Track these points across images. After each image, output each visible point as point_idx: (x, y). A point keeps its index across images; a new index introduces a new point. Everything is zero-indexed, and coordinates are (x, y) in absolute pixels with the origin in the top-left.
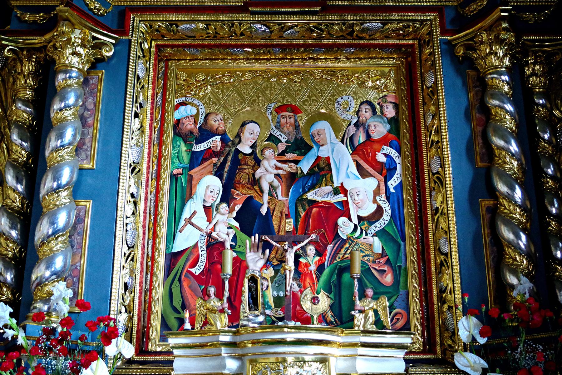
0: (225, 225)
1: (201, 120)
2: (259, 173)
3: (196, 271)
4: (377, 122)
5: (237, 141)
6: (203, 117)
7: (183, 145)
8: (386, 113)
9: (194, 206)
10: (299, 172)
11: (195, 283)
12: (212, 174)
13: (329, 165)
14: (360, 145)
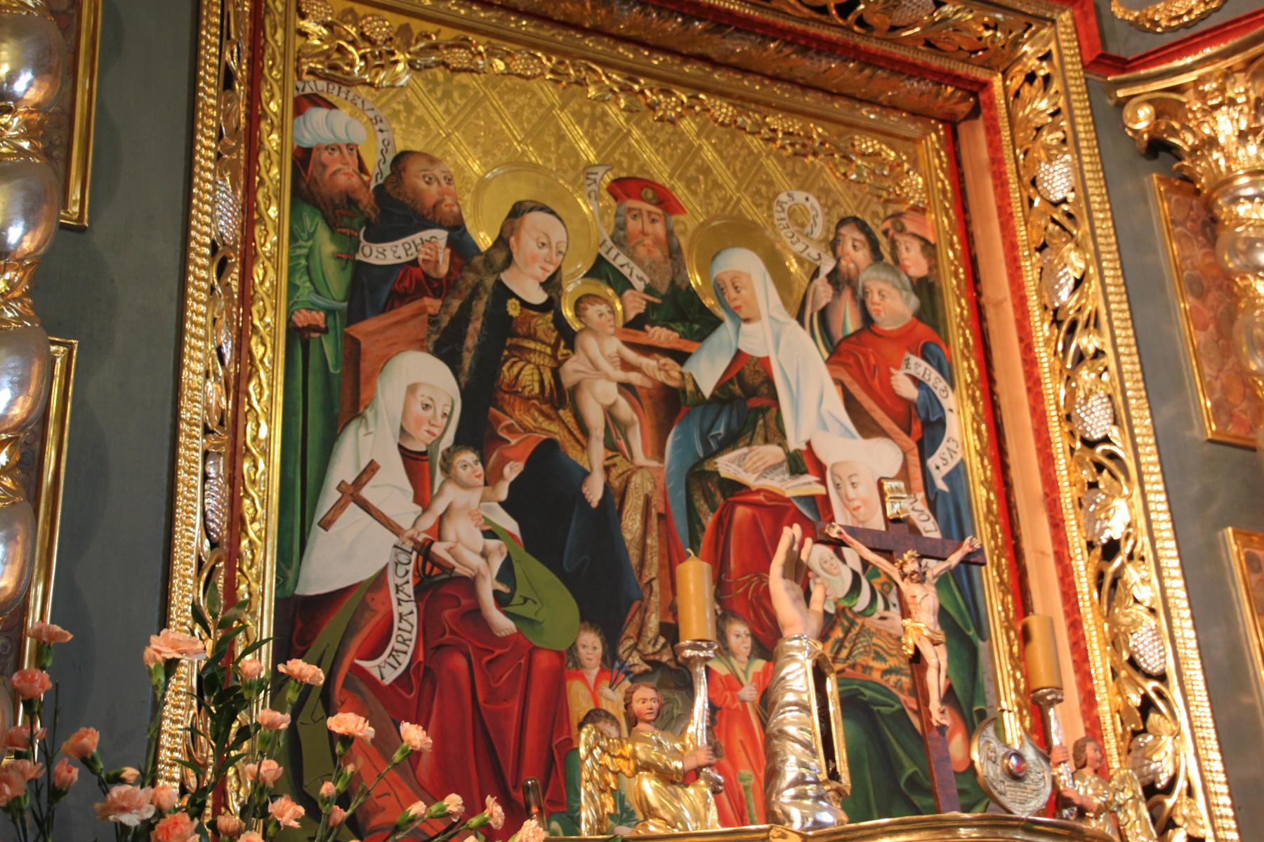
0: (475, 526)
2: (573, 369)
4: (886, 281)
5: (500, 257)
6: (390, 158)
8: (907, 263)
9: (367, 445)
10: (690, 388)
12: (423, 348)
13: (770, 382)
14: (847, 338)
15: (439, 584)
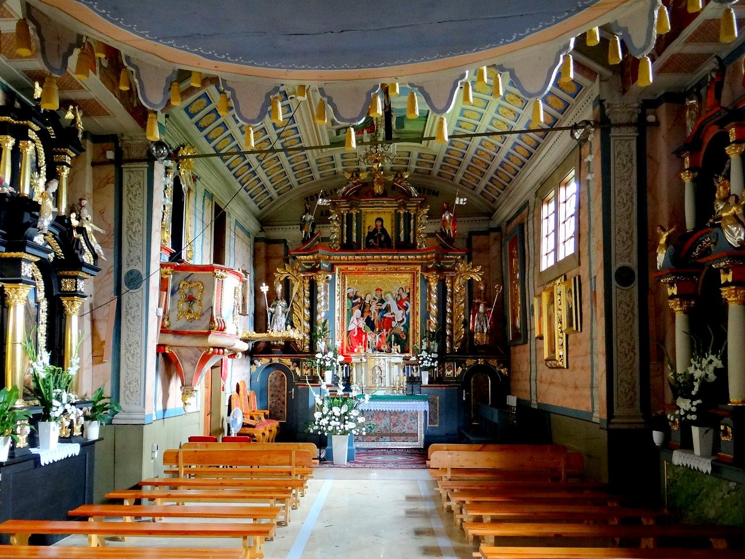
0: (362, 324)
1: (354, 294)
3: (355, 335)
9: (353, 318)
15: (359, 329)
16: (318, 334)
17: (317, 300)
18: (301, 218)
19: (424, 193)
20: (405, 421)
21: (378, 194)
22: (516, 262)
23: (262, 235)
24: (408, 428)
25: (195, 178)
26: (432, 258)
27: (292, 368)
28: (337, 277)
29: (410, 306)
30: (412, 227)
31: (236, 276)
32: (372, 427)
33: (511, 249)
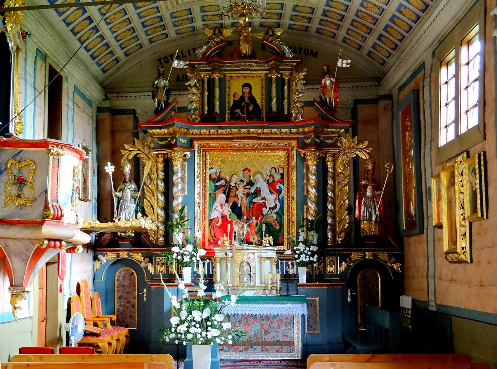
0: (227, 210)
1: (218, 174)
2: (237, 193)
3: (219, 225)
7: (212, 183)
9: (217, 204)
11: (218, 229)
15: (224, 217)
16: (175, 223)
17: (173, 182)
18: (153, 84)
19: (300, 53)
20: (279, 327)
21: (245, 55)
22: (410, 136)
23: (107, 104)
24: (283, 335)
25: (24, 35)
26: (310, 132)
27: (143, 265)
28: (196, 154)
29: (284, 189)
30: (286, 95)
31: (75, 154)
32: (240, 334)
33: (404, 120)
